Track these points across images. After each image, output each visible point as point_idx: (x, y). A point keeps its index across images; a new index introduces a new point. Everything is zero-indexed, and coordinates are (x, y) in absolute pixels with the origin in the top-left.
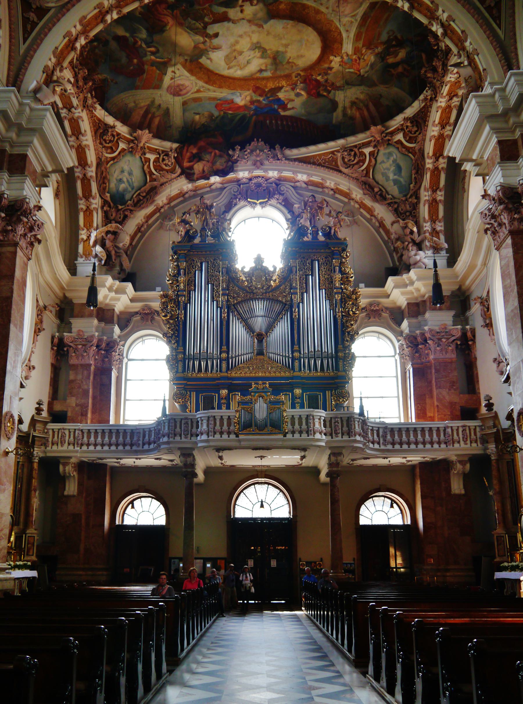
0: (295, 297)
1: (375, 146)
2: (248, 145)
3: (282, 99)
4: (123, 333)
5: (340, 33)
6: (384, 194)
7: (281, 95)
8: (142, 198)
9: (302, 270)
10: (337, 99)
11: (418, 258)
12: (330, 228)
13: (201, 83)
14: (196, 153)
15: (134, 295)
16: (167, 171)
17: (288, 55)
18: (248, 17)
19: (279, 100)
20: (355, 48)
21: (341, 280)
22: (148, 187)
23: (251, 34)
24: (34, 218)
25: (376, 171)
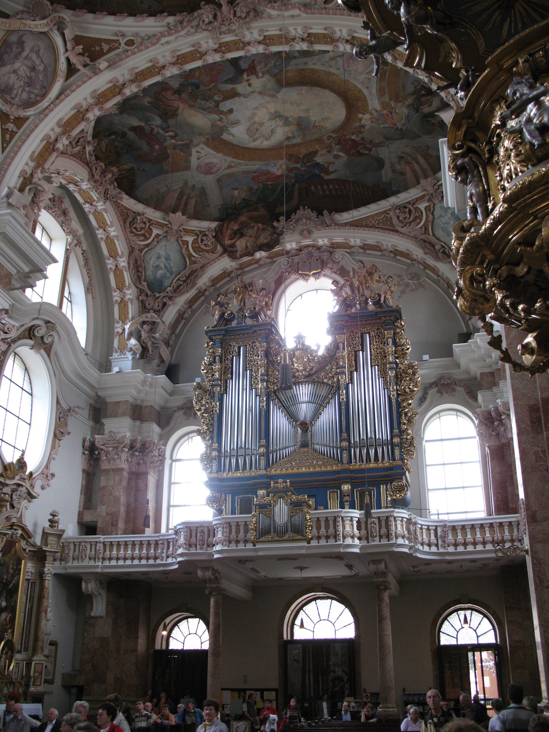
1: (430, 200)
3: (322, 163)
4: (164, 432)
5: (360, 91)
7: (318, 159)
8: (181, 283)
10: (380, 156)
12: (380, 296)
13: (229, 159)
14: (237, 230)
16: (208, 251)
17: (313, 119)
18: (258, 90)
19: (318, 164)
20: (382, 103)
21: (396, 353)
22: (187, 272)
23: (266, 105)
24: (3, 322)
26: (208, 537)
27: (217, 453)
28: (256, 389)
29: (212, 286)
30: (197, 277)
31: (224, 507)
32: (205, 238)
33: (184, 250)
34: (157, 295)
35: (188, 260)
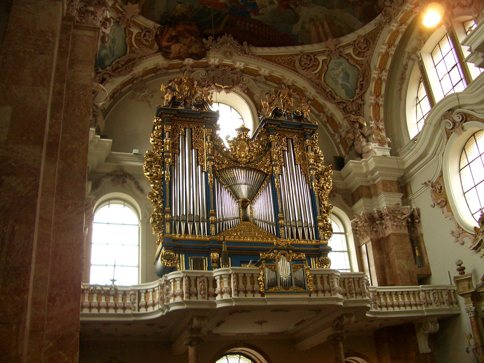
0: (276, 169)
1: (328, 55)
2: (219, 37)
6: (334, 94)
8: (120, 66)
10: (299, 14)
11: (370, 147)
12: (303, 113)
14: (174, 36)
16: (146, 46)
22: (126, 58)
26: (208, 286)
28: (202, 167)
29: (141, 77)
30: (134, 65)
31: (178, 266)
32: (147, 34)
33: (127, 39)
34: (100, 70)
35: (128, 48)
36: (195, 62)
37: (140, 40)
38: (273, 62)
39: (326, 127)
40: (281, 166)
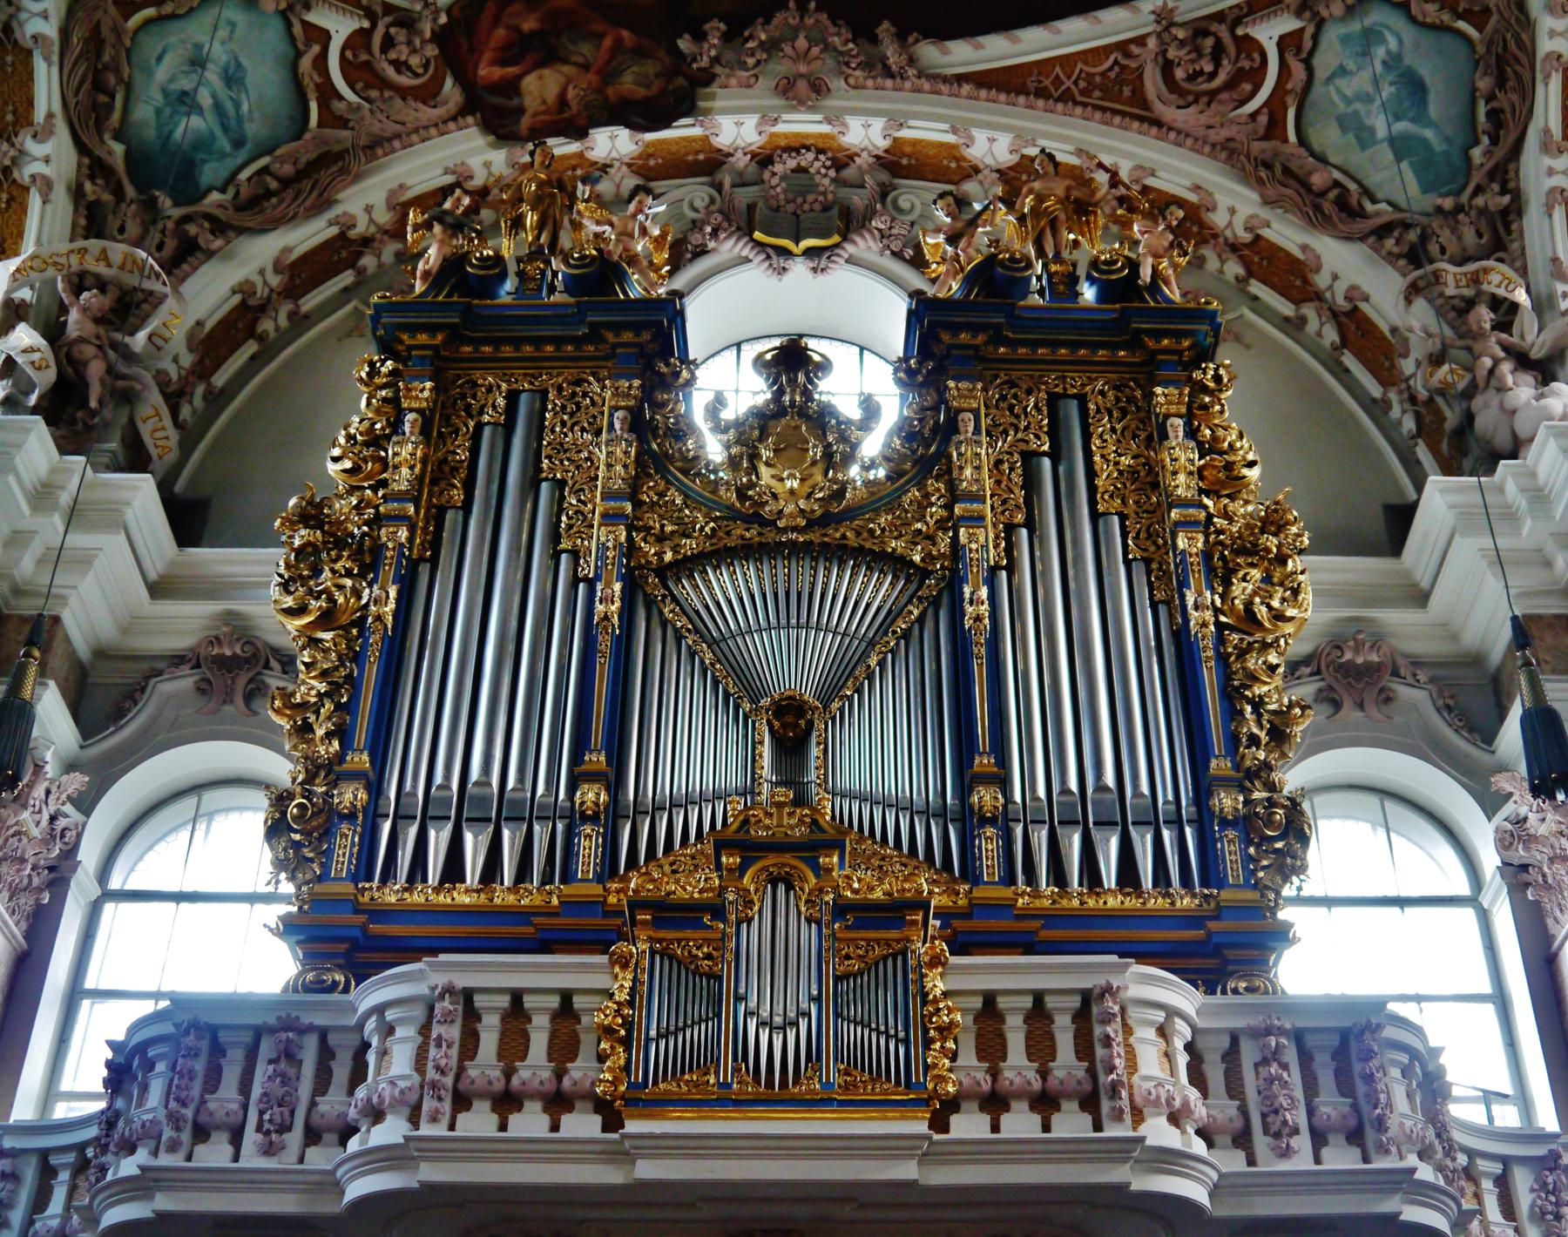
2: (760, 20)
6: (1354, 201)
8: (274, 185)
9: (1006, 432)
12: (1134, 266)
14: (533, 33)
15: (172, 564)
16: (403, 93)
22: (305, 149)
25: (1309, 115)
26: (322, 1083)
27: (362, 795)
28: (575, 554)
32: (399, 34)
33: (306, 63)
34: (165, 202)
35: (314, 106)
36: (648, 145)
37: (367, 66)
38: (1027, 94)
39: (1342, 374)
40: (1010, 529)
